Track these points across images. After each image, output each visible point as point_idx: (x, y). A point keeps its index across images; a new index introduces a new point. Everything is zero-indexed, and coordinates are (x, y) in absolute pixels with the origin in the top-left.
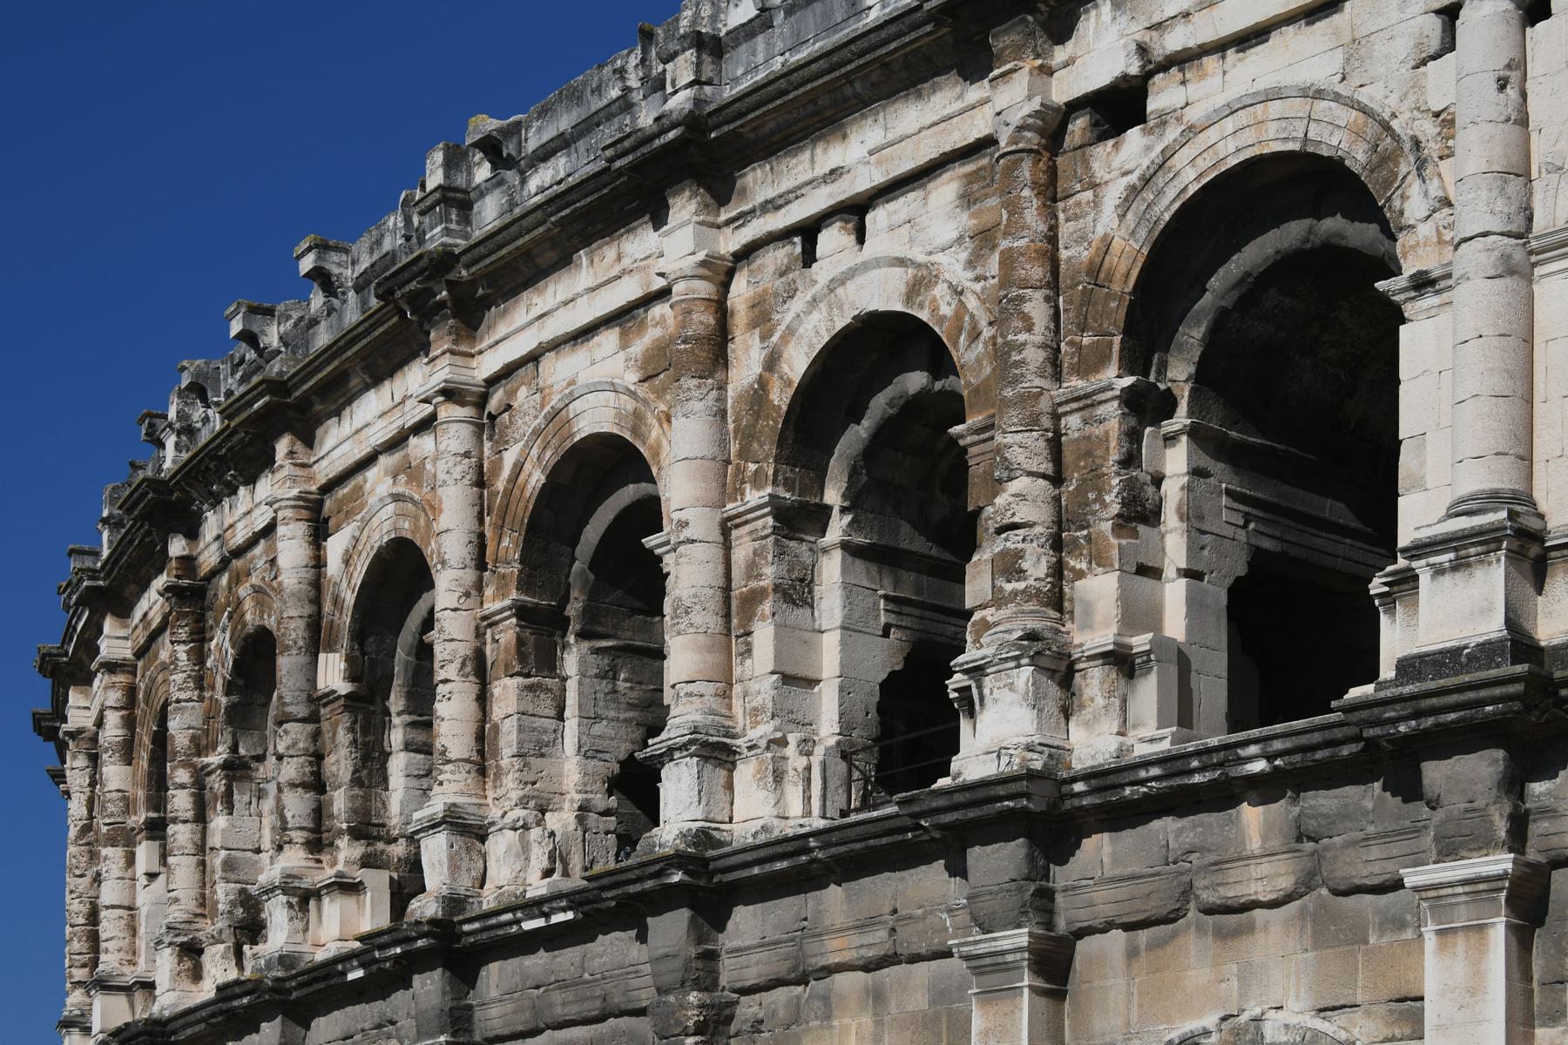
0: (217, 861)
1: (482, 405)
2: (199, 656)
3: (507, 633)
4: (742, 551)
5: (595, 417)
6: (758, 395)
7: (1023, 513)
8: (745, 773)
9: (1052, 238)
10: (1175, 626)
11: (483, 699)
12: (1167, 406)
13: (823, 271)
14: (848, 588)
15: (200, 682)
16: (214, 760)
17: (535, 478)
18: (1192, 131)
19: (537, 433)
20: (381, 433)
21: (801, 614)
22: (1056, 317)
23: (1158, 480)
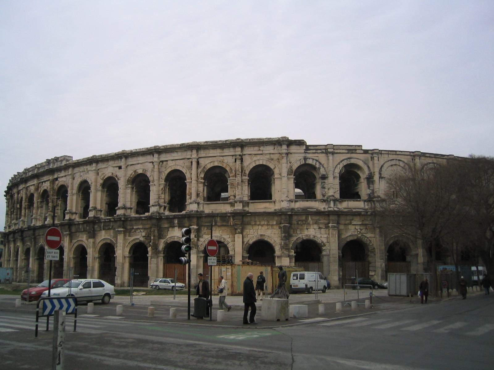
0: (12, 219)
1: (27, 188)
2: (12, 201)
3: (27, 207)
4: (39, 204)
5: (32, 192)
6: (40, 193)
7: (50, 206)
8: (38, 220)
9: (53, 187)
10: (59, 213)
11: (25, 211)
12: (59, 199)
13: (43, 185)
14: (45, 207)
15: (12, 203)
16: (12, 210)
17: (29, 195)
18: (60, 182)
19: (29, 192)
20: (21, 188)
21: (42, 209)
22: (53, 192)
23: (59, 203)
